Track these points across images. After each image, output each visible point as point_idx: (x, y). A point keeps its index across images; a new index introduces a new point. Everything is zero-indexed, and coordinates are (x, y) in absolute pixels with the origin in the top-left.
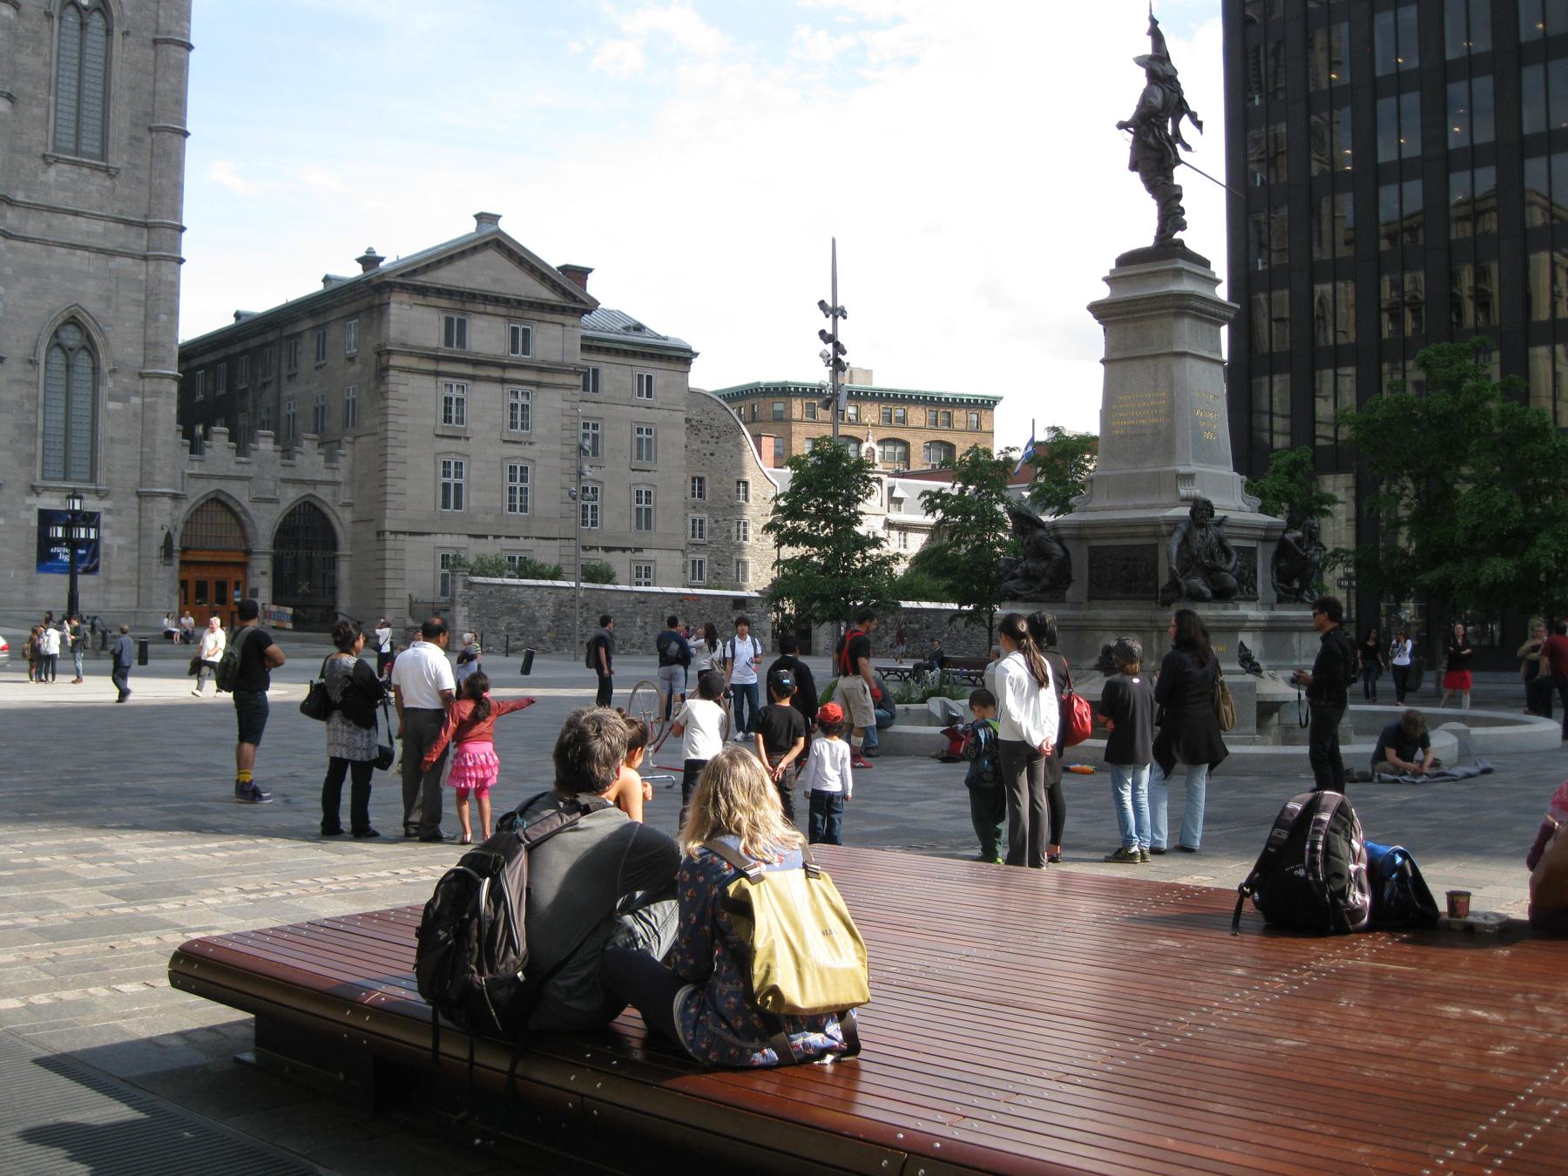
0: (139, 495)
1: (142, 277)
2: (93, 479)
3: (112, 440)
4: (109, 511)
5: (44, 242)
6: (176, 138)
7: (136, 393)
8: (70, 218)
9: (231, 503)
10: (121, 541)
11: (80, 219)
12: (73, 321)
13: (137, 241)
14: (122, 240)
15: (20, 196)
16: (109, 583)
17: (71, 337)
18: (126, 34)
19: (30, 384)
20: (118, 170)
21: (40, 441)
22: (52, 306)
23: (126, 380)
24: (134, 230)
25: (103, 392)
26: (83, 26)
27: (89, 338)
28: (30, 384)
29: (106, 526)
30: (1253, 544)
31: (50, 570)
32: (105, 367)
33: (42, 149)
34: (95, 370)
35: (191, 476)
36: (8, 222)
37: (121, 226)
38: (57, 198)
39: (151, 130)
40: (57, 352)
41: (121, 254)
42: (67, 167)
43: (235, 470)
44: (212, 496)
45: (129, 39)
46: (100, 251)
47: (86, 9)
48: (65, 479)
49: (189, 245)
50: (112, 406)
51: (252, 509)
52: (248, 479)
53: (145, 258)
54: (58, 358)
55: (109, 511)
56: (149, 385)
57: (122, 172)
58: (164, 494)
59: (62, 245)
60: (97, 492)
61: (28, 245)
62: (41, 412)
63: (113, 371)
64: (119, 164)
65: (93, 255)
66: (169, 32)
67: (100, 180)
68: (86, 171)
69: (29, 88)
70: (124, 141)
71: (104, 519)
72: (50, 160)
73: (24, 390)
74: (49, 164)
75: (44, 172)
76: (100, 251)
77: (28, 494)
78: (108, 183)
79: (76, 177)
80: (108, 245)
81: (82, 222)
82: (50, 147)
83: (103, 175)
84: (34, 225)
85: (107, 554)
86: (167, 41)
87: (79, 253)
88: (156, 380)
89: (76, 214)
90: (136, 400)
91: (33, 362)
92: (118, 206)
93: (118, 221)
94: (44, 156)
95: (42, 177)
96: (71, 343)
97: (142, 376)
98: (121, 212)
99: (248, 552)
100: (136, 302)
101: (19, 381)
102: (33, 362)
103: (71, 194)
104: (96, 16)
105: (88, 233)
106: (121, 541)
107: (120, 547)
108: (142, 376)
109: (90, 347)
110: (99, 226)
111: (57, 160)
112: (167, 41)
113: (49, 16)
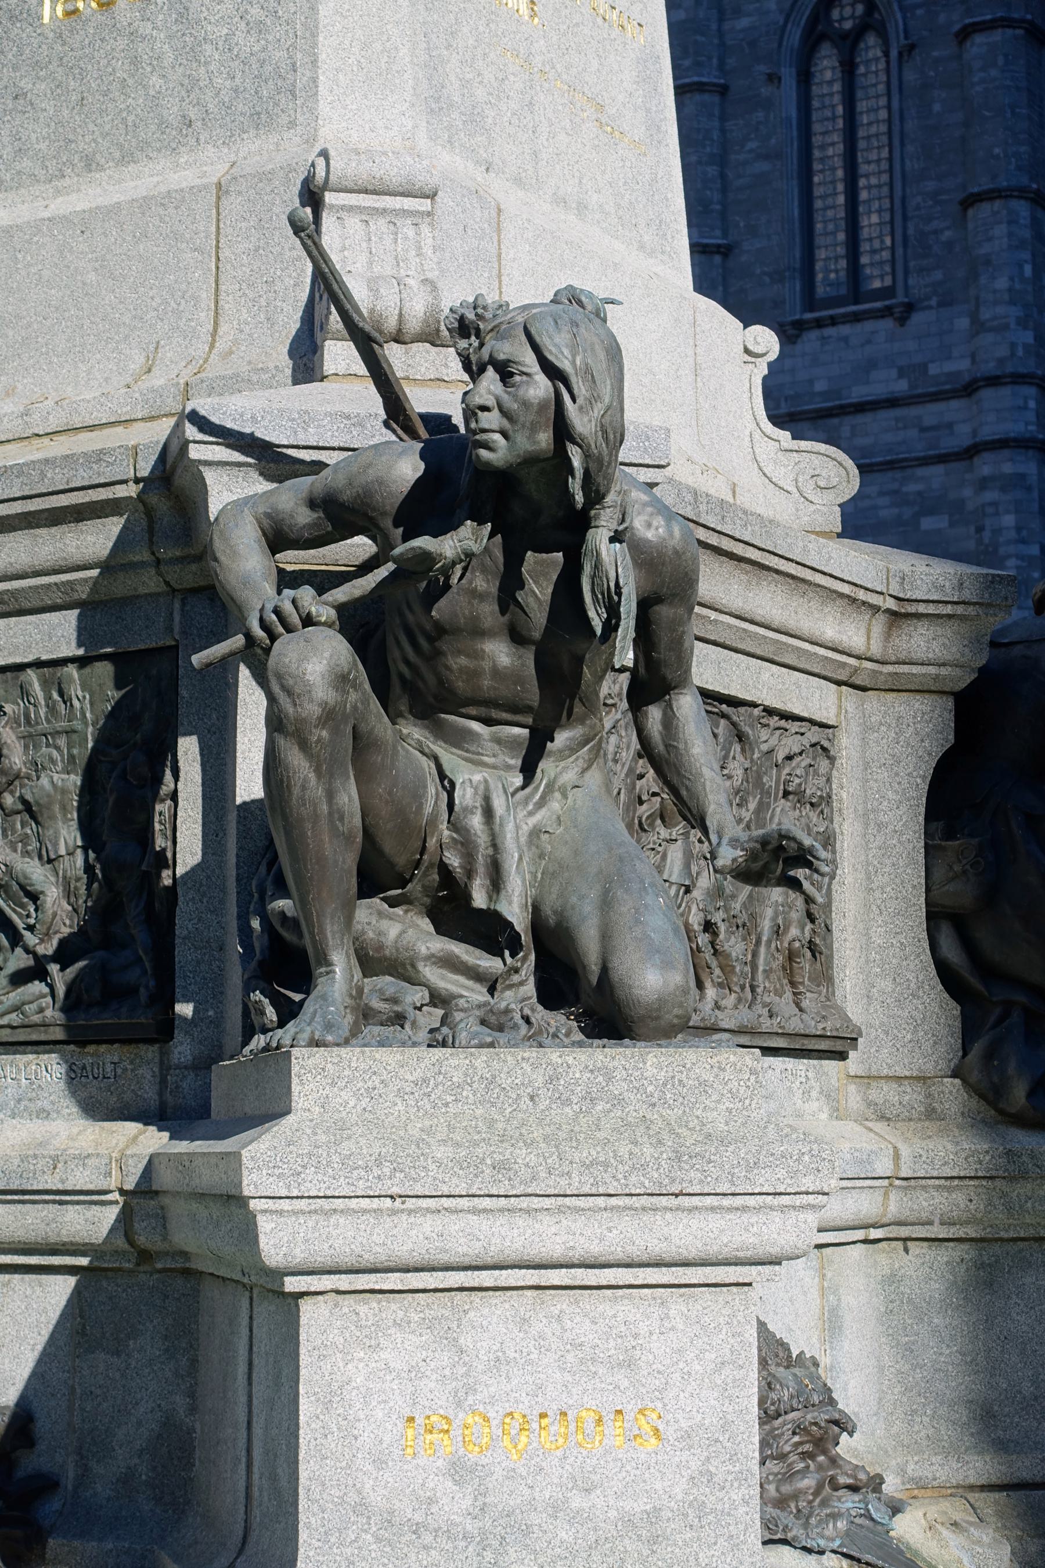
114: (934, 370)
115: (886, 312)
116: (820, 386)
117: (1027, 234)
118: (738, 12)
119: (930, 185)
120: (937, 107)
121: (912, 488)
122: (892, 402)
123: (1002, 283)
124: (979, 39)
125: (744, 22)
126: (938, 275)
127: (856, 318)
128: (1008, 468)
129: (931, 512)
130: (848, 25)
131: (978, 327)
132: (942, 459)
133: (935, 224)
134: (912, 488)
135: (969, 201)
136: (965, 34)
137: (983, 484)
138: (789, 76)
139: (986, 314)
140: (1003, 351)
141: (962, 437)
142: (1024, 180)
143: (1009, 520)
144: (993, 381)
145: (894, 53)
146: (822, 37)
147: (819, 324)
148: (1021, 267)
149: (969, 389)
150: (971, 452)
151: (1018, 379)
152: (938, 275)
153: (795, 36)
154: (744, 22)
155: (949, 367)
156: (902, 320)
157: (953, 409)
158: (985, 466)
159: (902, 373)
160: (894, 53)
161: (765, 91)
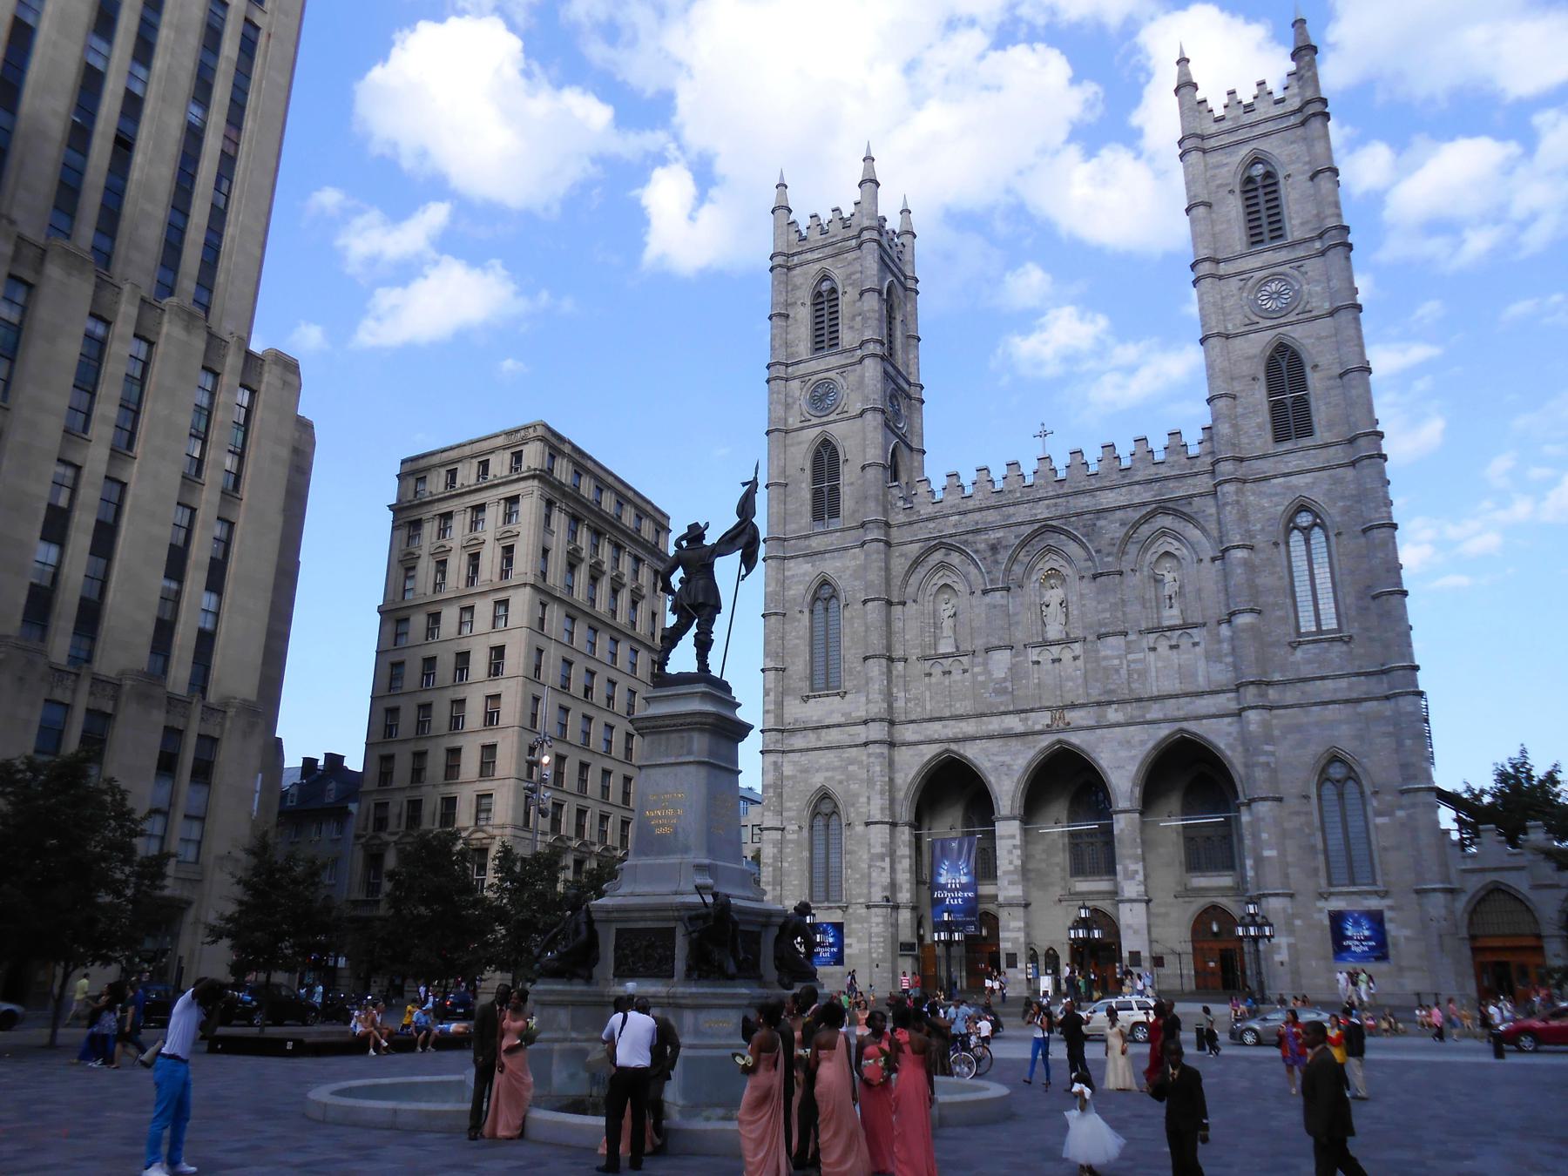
0: (1418, 892)
1: (1388, 713)
2: (1374, 883)
3: (1385, 849)
4: (1391, 908)
5: (1300, 706)
6: (1395, 599)
7: (1401, 807)
8: (1318, 683)
9: (1512, 892)
10: (1408, 932)
11: (1326, 681)
12: (1334, 758)
13: (1381, 686)
14: (1364, 688)
15: (1277, 677)
16: (1401, 969)
17: (1337, 771)
18: (1339, 534)
19: (1307, 813)
20: (1351, 637)
21: (1321, 858)
22: (1314, 751)
23: (1389, 798)
24: (1374, 679)
25: (1369, 809)
26: (1307, 541)
27: (1351, 768)
28: (1307, 813)
29: (1391, 920)
30: (672, 924)
31: (1343, 959)
32: (1368, 790)
33: (1288, 639)
34: (1362, 794)
35: (1465, 871)
36: (1271, 697)
37: (1363, 678)
38: (1306, 671)
39: (1374, 598)
40: (1328, 785)
41: (1365, 700)
42: (1310, 646)
43: (1509, 862)
44: (1491, 887)
45: (1343, 537)
46: (1347, 701)
47: (1305, 528)
48: (1353, 883)
49: (1424, 681)
50: (1379, 820)
51: (1535, 897)
52: (1522, 868)
53: (1387, 698)
54: (1329, 791)
55: (1391, 908)
56: (1406, 800)
57: (1355, 637)
58: (1434, 890)
59: (1315, 704)
60: (1376, 893)
61: (1289, 711)
62: (1319, 834)
63: (1376, 793)
64: (1352, 631)
65: (1342, 706)
66: (1371, 521)
67: (1338, 648)
68: (1326, 645)
69: (1271, 599)
70: (1353, 613)
71: (1388, 914)
72: (1294, 645)
73: (1303, 819)
74: (1295, 648)
75: (1293, 655)
76: (1347, 701)
77: (1319, 900)
78: (1345, 648)
79: (1317, 651)
80: (1354, 695)
81: (1329, 684)
82: (1294, 635)
83: (1340, 644)
84: (1291, 696)
85: (1395, 945)
86: (1371, 528)
87: (1330, 706)
88: (1412, 795)
89: (1322, 678)
90: (1400, 814)
91: (1307, 797)
92: (1357, 663)
93: (1358, 674)
94: (1290, 644)
95: (1291, 659)
96: (1338, 776)
97: (1403, 792)
98: (1361, 667)
99: (1539, 937)
100: (1389, 734)
101: (1298, 813)
102: (1307, 797)
103: (1316, 665)
104: (1316, 529)
105: (1335, 690)
106: (1408, 932)
107: (1407, 938)
108: (1403, 792)
109: (1352, 776)
110: (1344, 683)
111: (1300, 643)
112: (1371, 528)
113: (1276, 544)
114: (853, 715)
115: (838, 694)
116: (815, 718)
117: (885, 670)
118: (790, 589)
119: (853, 651)
120: (856, 625)
121: (846, 755)
122: (839, 725)
123: (877, 687)
124: (870, 604)
125: (792, 592)
126: (855, 682)
127: (828, 695)
128: (878, 751)
129: (851, 764)
130: (826, 596)
131: (868, 701)
132: (856, 746)
133: (855, 665)
134: (846, 755)
135: (866, 659)
136: (865, 602)
137: (869, 755)
138: (807, 612)
139: (870, 697)
140: (877, 710)
141: (862, 740)
142: (885, 652)
143: (878, 768)
144: (873, 720)
145: (842, 606)
146: (818, 598)
147: (815, 697)
148: (882, 681)
149: (865, 722)
150: (866, 744)
151: (882, 720)
152: (855, 682)
153: (809, 598)
154: (792, 592)
155: (859, 714)
156: (843, 697)
157: (862, 728)
158: (872, 749)
159: (843, 715)
160: (842, 606)
161: (799, 615)
